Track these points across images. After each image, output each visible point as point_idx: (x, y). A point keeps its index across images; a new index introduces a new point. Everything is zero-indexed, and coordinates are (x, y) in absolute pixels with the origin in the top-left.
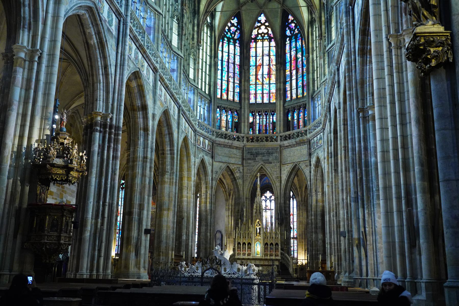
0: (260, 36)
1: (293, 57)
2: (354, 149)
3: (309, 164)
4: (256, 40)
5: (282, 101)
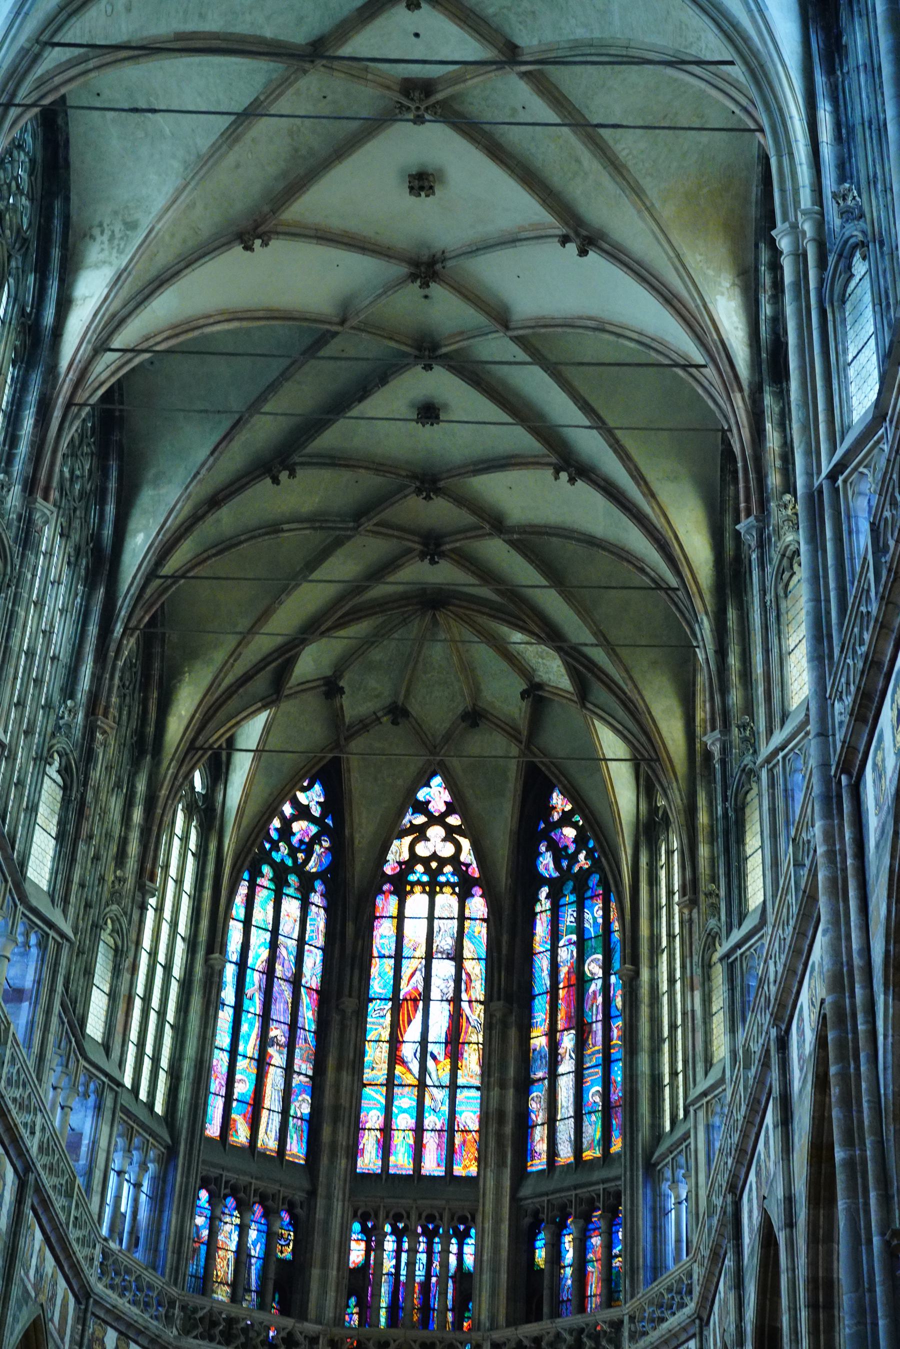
0: (420, 868)
1: (563, 971)
4: (401, 887)
5: (507, 1172)
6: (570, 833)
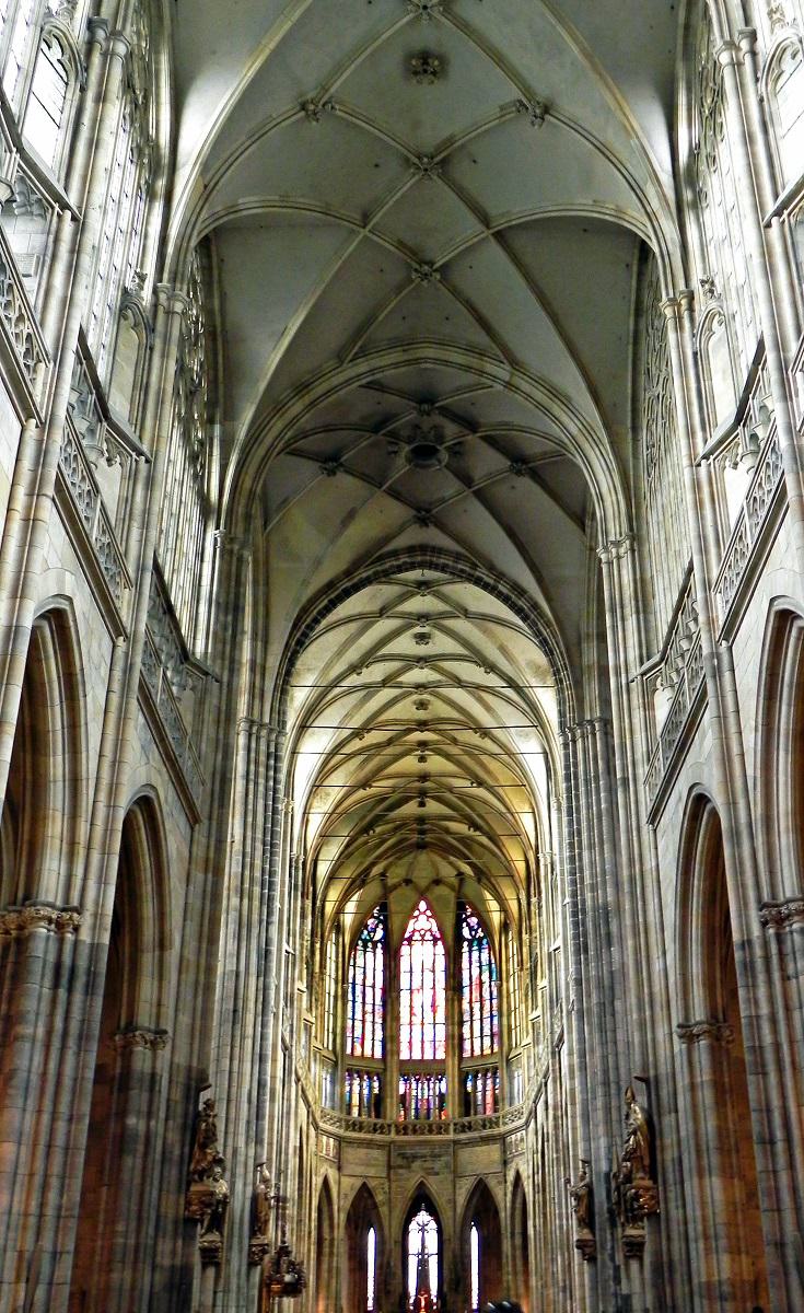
0: (417, 934)
2: (561, 1226)
3: (501, 1179)
4: (410, 940)
6: (474, 921)
